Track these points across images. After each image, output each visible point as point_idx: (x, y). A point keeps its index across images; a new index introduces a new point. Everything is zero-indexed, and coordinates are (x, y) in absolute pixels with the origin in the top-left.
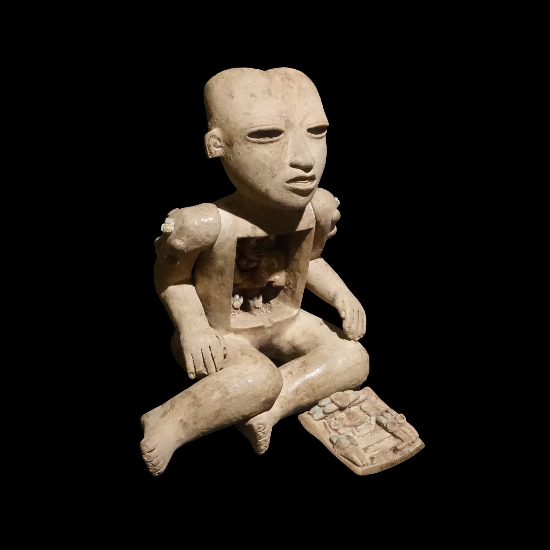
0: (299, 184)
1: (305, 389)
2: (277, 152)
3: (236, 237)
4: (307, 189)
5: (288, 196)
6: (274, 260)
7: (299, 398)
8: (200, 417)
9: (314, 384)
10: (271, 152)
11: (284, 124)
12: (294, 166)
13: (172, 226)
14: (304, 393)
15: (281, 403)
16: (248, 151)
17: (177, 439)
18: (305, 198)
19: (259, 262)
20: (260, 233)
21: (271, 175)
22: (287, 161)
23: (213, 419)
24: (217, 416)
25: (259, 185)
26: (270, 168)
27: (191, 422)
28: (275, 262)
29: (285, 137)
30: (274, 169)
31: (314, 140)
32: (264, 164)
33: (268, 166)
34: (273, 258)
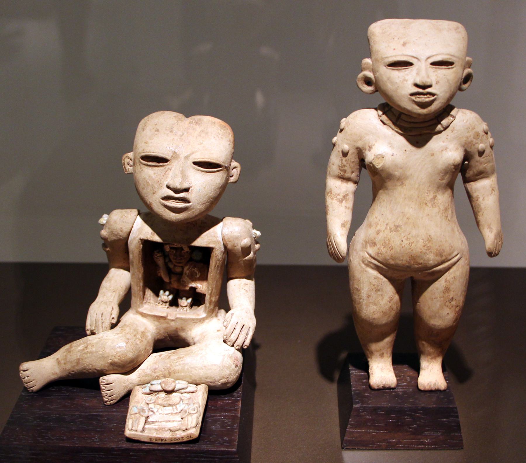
0: (171, 202)
1: (163, 370)
2: (160, 175)
3: (139, 238)
4: (174, 207)
5: (162, 210)
6: (196, 270)
7: (156, 375)
8: (68, 360)
9: (171, 368)
10: (155, 174)
11: (171, 155)
12: (168, 187)
13: (105, 220)
14: (161, 373)
15: (139, 374)
16: (140, 170)
17: (54, 372)
18: (177, 214)
19: (183, 268)
20: (157, 238)
21: (152, 192)
22: (166, 183)
23: (75, 364)
24: (78, 363)
25: (146, 198)
26: (152, 186)
27: (63, 362)
28: (197, 272)
29: (170, 165)
30: (154, 187)
31: (200, 172)
32: (148, 182)
33: (151, 184)
34: (196, 269)
